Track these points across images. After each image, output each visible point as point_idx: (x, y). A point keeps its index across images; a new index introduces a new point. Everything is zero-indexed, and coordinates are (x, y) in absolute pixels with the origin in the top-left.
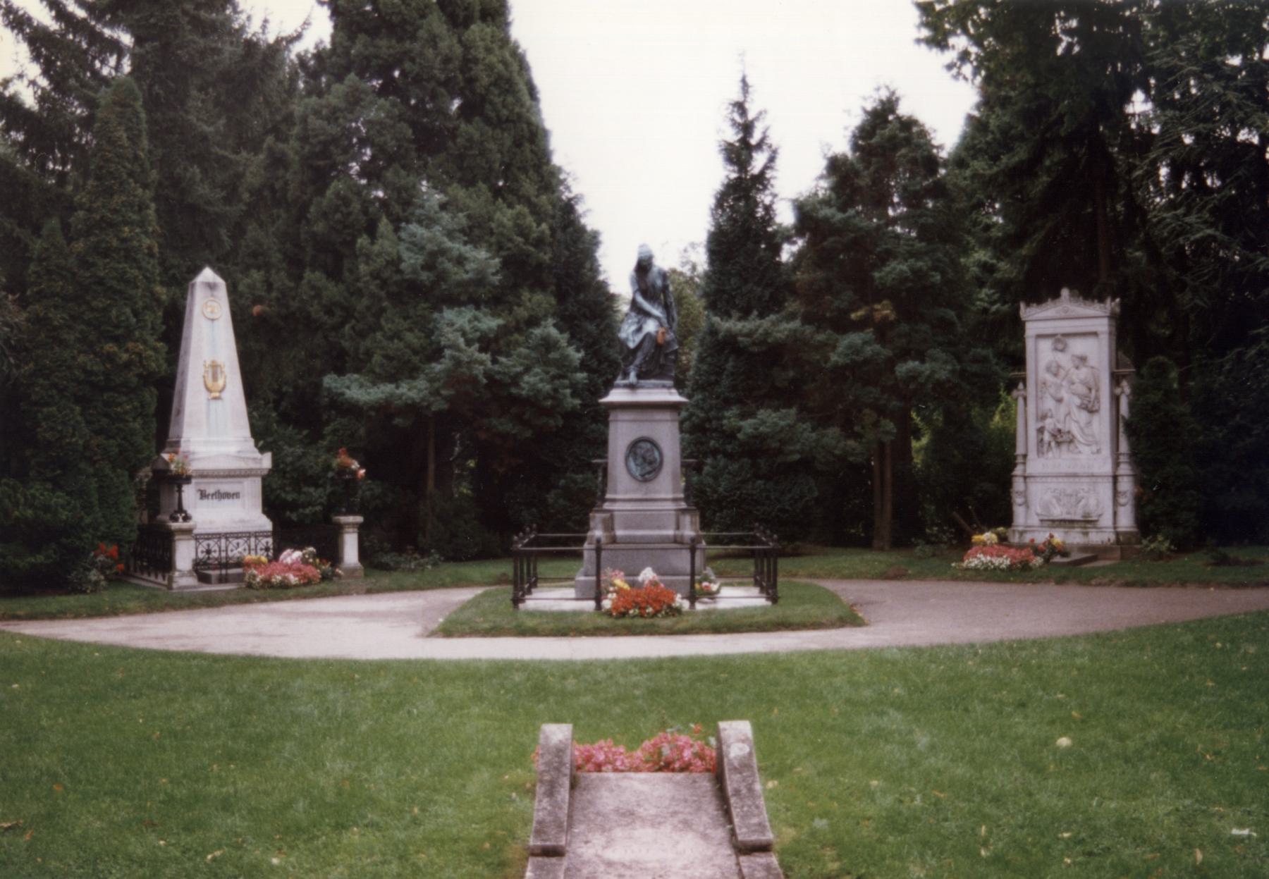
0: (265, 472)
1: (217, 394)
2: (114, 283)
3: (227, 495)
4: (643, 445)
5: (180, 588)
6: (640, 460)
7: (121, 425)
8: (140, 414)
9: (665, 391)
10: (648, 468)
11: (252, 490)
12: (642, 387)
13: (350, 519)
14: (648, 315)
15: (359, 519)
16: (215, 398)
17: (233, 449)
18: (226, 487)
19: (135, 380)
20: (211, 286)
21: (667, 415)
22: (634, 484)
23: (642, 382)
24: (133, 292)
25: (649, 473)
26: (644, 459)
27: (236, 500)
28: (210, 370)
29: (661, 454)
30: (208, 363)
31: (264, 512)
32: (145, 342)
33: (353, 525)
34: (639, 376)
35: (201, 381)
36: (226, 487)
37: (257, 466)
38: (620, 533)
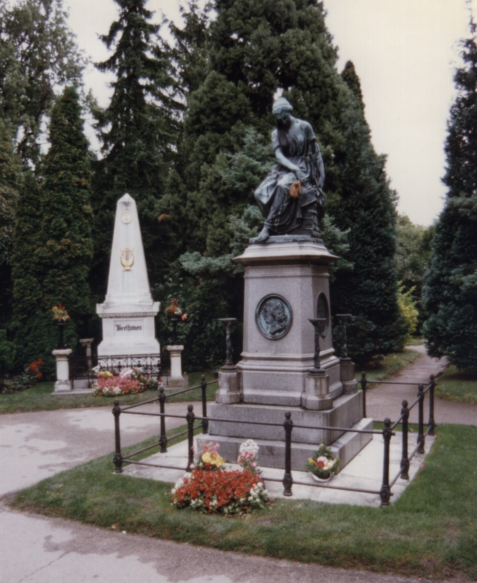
0: (156, 314)
1: (128, 268)
2: (55, 205)
3: (134, 328)
4: (272, 301)
5: (59, 391)
6: (270, 318)
7: (61, 288)
8: (75, 281)
9: (296, 245)
10: (278, 326)
11: (149, 324)
12: (273, 243)
13: (175, 347)
14: (287, 170)
15: (181, 347)
16: (128, 270)
17: (137, 301)
19: (66, 261)
20: (126, 204)
21: (297, 271)
22: (265, 343)
23: (273, 238)
24: (65, 209)
25: (279, 331)
26: (274, 316)
27: (139, 331)
29: (291, 312)
30: (124, 249)
32: (73, 238)
33: (177, 351)
34: (272, 232)
36: (133, 323)
37: (150, 311)
38: (247, 392)
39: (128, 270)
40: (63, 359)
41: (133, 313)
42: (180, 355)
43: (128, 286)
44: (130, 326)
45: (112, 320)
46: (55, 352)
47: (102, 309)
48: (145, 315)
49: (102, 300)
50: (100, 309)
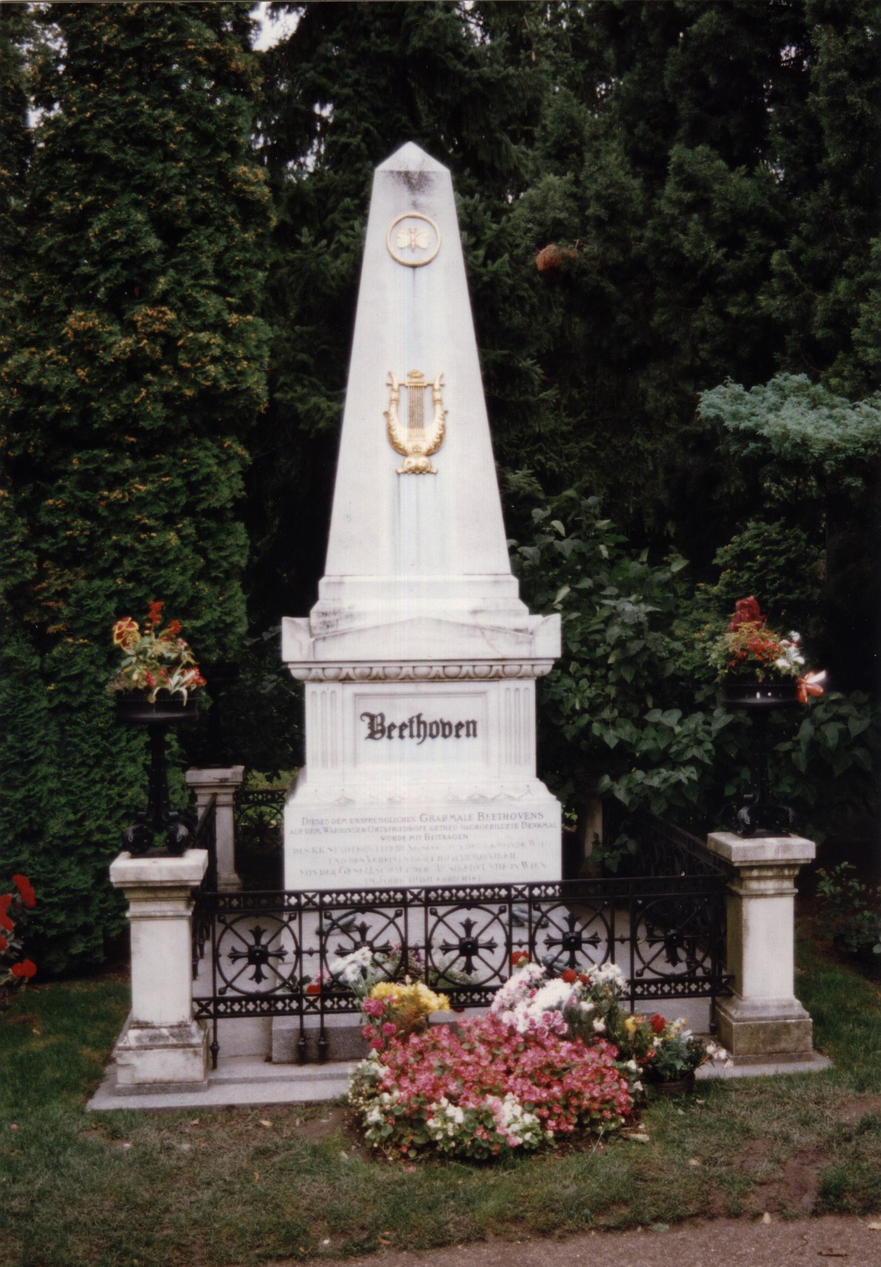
0: (546, 668)
1: (422, 461)
2: (106, 147)
3: (444, 729)
5: (142, 1088)
7: (127, 540)
8: (189, 510)
11: (510, 715)
13: (771, 848)
15: (801, 848)
16: (417, 471)
17: (459, 606)
18: (441, 704)
19: (158, 411)
20: (413, 182)
24: (156, 168)
27: (465, 742)
30: (400, 378)
31: (543, 773)
32: (189, 307)
33: (778, 868)
36: (441, 704)
37: (523, 651)
39: (417, 471)
40: (167, 908)
41: (459, 661)
42: (788, 885)
43: (420, 541)
44: (427, 718)
45: (350, 689)
46: (124, 867)
47: (306, 640)
48: (496, 673)
49: (302, 601)
50: (295, 641)
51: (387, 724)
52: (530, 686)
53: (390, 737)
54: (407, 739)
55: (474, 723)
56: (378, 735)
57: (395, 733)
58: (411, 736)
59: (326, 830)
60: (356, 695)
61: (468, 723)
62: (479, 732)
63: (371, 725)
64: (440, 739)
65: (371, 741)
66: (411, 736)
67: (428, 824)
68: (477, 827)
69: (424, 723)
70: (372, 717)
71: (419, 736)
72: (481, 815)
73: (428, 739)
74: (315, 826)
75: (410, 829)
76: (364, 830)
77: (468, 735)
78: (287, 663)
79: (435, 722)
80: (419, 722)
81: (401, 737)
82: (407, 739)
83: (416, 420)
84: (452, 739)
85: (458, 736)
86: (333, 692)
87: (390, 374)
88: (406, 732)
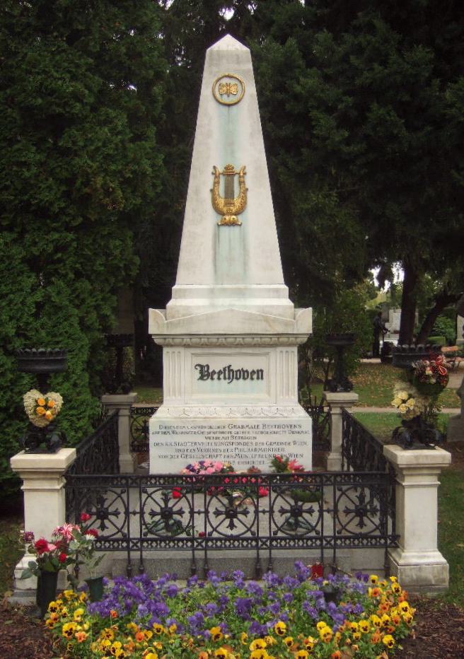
3: (243, 374)
11: (283, 369)
15: (440, 455)
28: (222, 180)
30: (220, 169)
31: (300, 401)
35: (208, 196)
42: (435, 481)
44: (235, 368)
46: (21, 460)
49: (161, 297)
50: (157, 322)
51: (210, 371)
52: (295, 350)
53: (212, 379)
54: (222, 380)
55: (262, 371)
56: (205, 378)
57: (215, 376)
58: (225, 378)
59: (173, 433)
60: (192, 354)
61: (258, 371)
62: (264, 377)
63: (201, 372)
64: (241, 380)
65: (200, 381)
66: (225, 378)
67: (234, 430)
68: (262, 433)
69: (232, 370)
70: (202, 367)
71: (229, 378)
72: (264, 426)
73: (235, 380)
74: (166, 430)
75: (223, 433)
76: (195, 433)
77: (258, 378)
78: (151, 335)
79: (239, 370)
80: (230, 370)
81: (219, 379)
82: (222, 380)
83: (229, 193)
84: (249, 380)
85: (252, 379)
86: (179, 352)
87: (215, 167)
88: (222, 376)
